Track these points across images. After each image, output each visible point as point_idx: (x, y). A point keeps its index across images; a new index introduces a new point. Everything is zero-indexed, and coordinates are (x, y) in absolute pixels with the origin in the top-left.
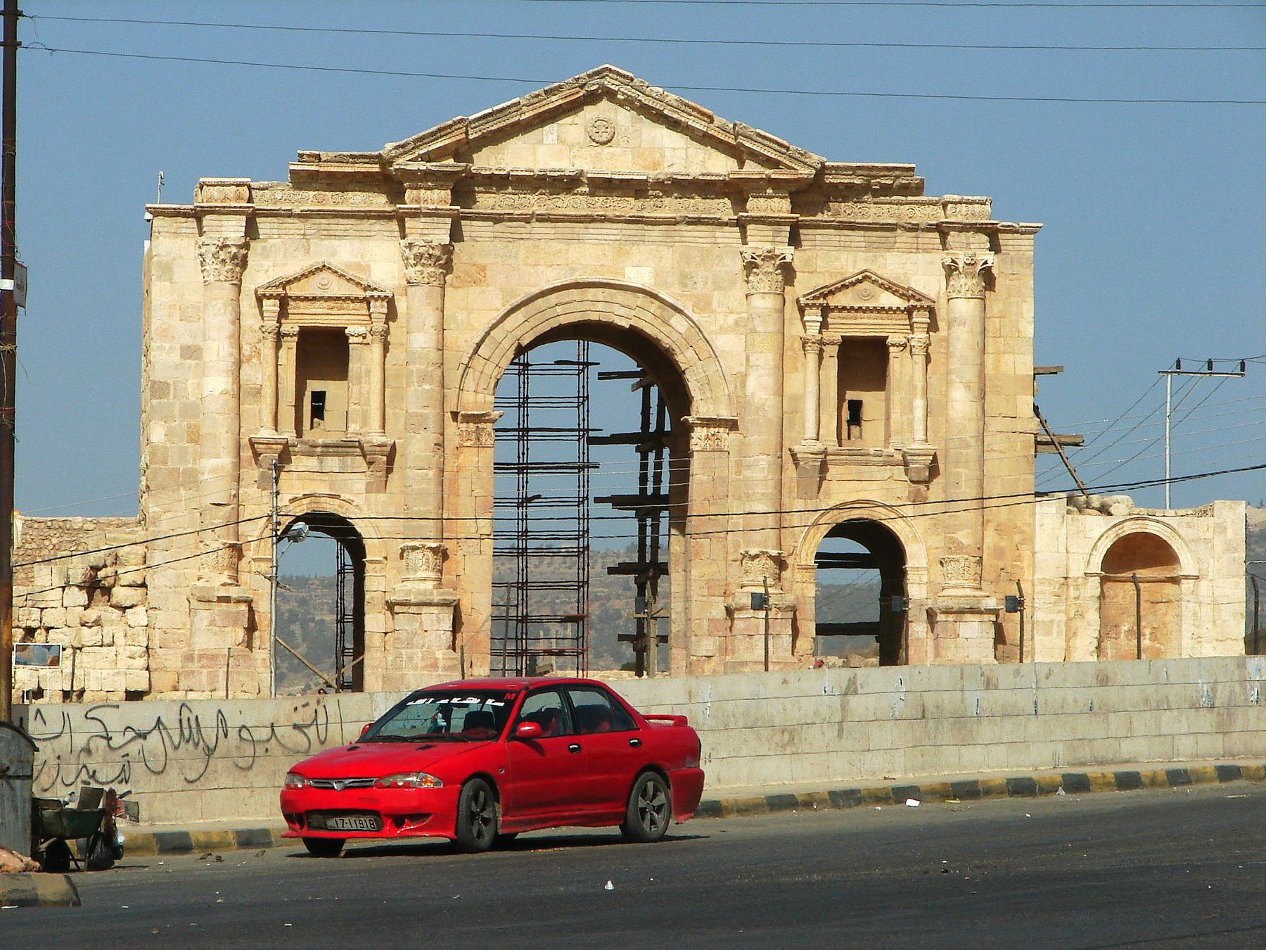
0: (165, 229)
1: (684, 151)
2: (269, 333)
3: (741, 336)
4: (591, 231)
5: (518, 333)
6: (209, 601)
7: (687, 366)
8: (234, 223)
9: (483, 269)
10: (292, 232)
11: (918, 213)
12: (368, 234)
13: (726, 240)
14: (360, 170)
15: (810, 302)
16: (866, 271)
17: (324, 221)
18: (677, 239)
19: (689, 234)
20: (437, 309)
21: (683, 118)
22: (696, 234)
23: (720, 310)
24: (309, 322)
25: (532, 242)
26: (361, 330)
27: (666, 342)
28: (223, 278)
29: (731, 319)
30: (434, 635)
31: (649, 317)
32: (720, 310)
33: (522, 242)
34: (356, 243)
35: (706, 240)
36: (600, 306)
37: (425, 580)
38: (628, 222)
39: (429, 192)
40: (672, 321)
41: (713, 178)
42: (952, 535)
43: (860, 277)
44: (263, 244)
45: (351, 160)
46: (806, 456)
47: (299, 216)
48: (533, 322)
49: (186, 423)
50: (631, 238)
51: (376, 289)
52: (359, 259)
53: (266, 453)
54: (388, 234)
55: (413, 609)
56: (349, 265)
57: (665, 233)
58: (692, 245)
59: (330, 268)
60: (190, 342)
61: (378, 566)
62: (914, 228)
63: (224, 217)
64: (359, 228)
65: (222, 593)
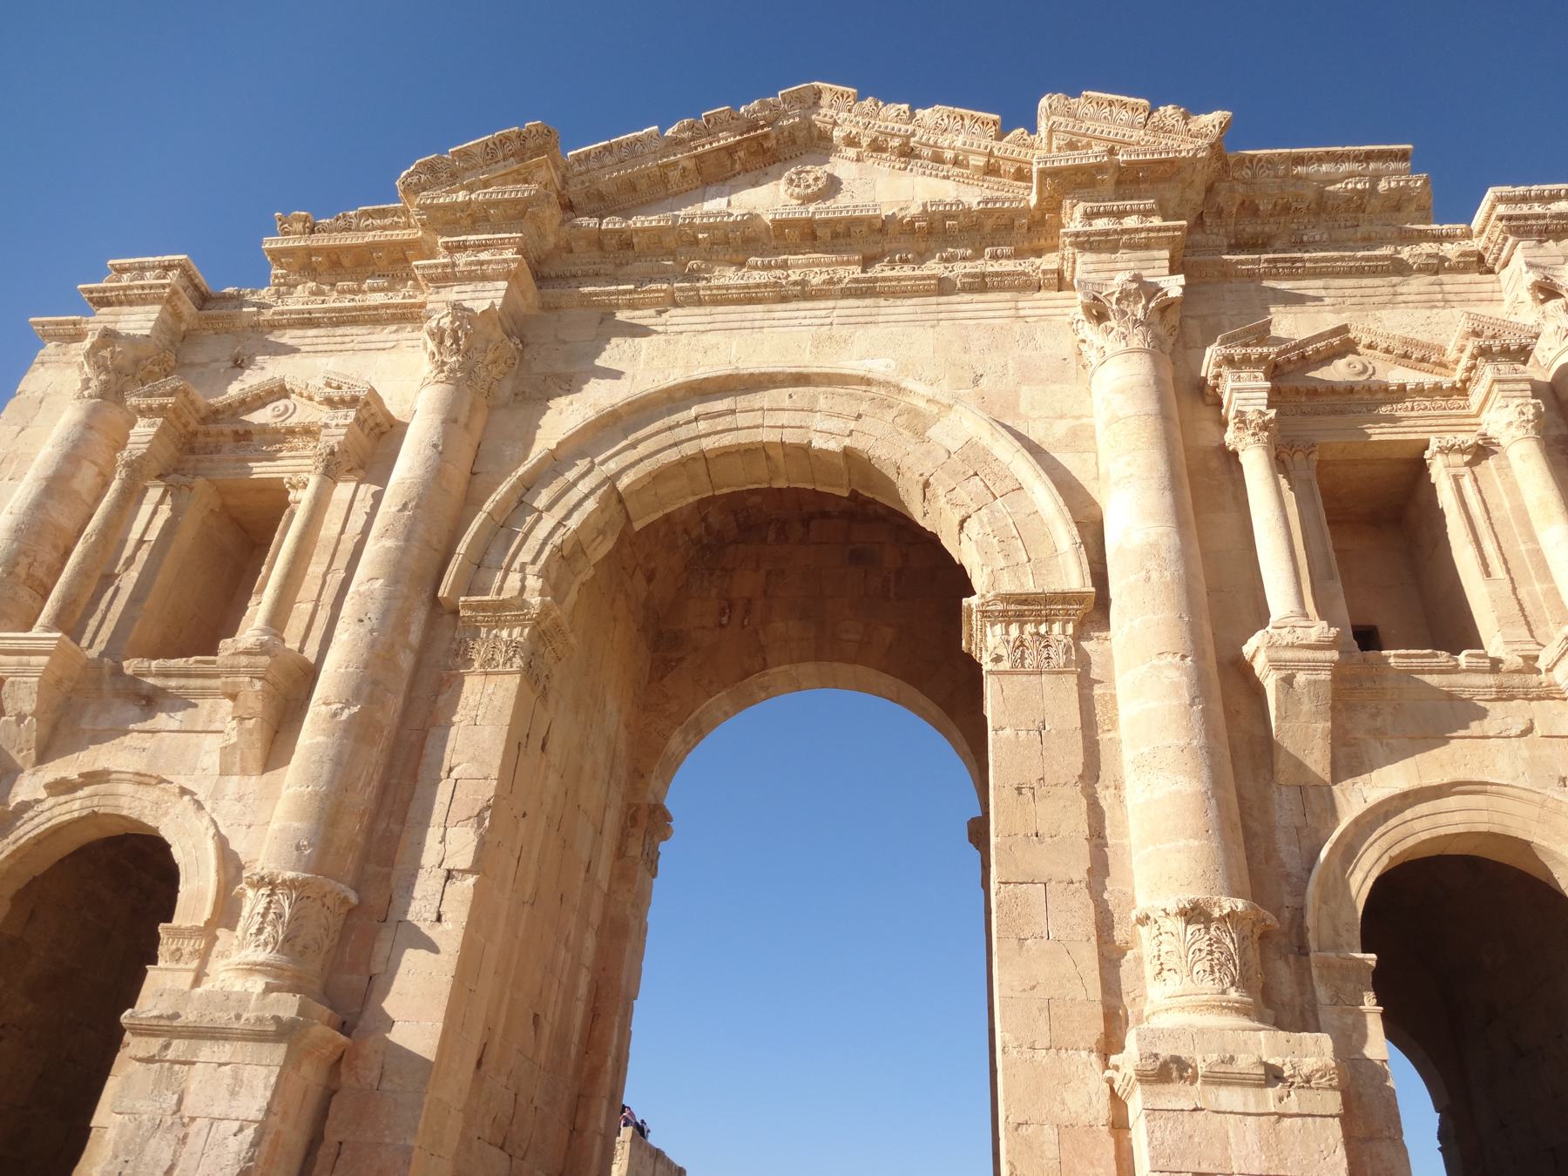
0: (53, 358)
3: (1085, 456)
4: (777, 315)
5: (612, 466)
8: (138, 317)
15: (1238, 352)
16: (1343, 329)
18: (941, 316)
21: (944, 141)
25: (662, 337)
29: (1061, 428)
36: (784, 418)
37: (252, 969)
38: (847, 294)
41: (1006, 205)
43: (1336, 341)
45: (363, 223)
46: (1288, 654)
48: (642, 449)
50: (852, 320)
51: (339, 388)
53: (14, 674)
55: (178, 1048)
57: (918, 309)
61: (188, 946)
62: (1437, 267)
63: (126, 309)
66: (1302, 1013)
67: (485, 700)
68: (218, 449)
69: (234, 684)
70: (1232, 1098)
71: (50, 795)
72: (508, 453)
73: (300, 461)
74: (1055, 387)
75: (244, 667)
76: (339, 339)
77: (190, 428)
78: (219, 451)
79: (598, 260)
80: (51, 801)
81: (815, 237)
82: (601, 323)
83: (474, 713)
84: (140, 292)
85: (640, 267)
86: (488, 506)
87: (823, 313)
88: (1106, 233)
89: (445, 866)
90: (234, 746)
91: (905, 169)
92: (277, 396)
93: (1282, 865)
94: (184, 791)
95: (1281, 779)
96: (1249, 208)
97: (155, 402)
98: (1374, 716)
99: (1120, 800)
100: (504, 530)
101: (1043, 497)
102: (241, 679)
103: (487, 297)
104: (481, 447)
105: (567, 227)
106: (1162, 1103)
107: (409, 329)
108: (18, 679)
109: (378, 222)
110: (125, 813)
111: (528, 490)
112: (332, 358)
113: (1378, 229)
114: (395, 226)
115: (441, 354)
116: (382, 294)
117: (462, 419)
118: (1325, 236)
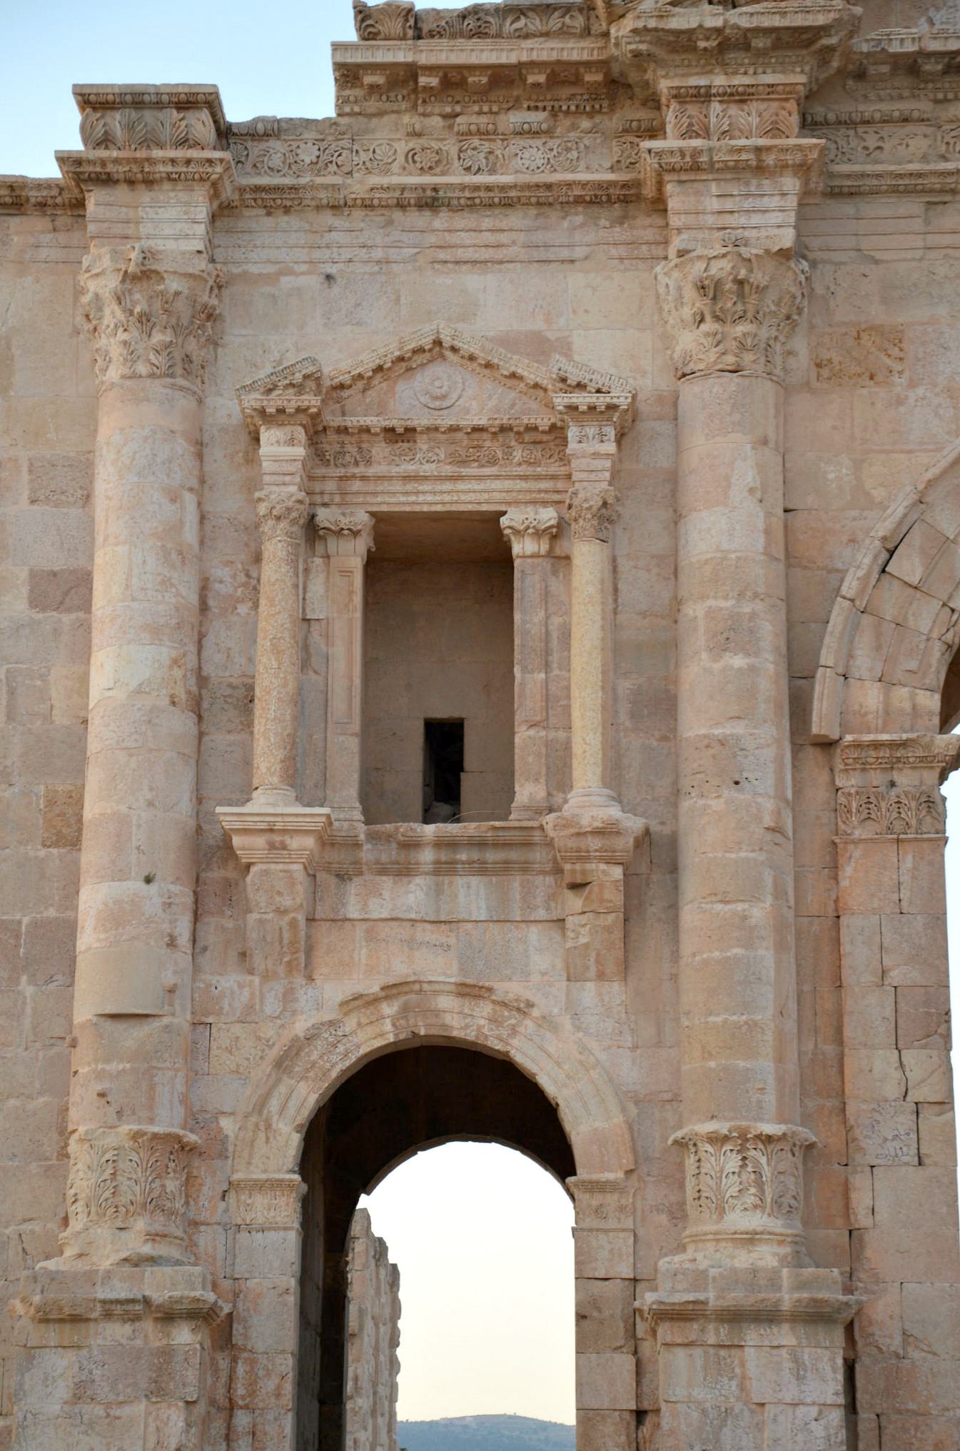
2: (278, 518)
6: (76, 1319)
8: (173, 213)
9: (893, 338)
10: (346, 254)
12: (565, 254)
14: (535, 56)
20: (765, 442)
24: (399, 499)
26: (548, 516)
28: (142, 368)
39: (733, 110)
44: (268, 289)
45: (508, 27)
47: (368, 206)
51: (580, 386)
52: (539, 325)
54: (622, 251)
56: (509, 342)
59: (454, 349)
60: (58, 562)
61: (611, 1200)
63: (145, 196)
64: (539, 237)
65: (120, 1290)
69: (584, 872)
71: (346, 1014)
72: (832, 476)
73: (507, 484)
75: (596, 851)
76: (489, 238)
78: (369, 462)
79: (906, 93)
80: (350, 1024)
83: (896, 897)
84: (169, 169)
86: (850, 586)
89: (914, 1096)
90: (586, 946)
94: (530, 1005)
97: (291, 401)
100: (866, 620)
102: (593, 866)
104: (788, 465)
107: (603, 222)
108: (273, 866)
109: (535, 24)
110: (455, 1034)
111: (891, 553)
112: (489, 276)
114: (563, 33)
116: (539, 142)
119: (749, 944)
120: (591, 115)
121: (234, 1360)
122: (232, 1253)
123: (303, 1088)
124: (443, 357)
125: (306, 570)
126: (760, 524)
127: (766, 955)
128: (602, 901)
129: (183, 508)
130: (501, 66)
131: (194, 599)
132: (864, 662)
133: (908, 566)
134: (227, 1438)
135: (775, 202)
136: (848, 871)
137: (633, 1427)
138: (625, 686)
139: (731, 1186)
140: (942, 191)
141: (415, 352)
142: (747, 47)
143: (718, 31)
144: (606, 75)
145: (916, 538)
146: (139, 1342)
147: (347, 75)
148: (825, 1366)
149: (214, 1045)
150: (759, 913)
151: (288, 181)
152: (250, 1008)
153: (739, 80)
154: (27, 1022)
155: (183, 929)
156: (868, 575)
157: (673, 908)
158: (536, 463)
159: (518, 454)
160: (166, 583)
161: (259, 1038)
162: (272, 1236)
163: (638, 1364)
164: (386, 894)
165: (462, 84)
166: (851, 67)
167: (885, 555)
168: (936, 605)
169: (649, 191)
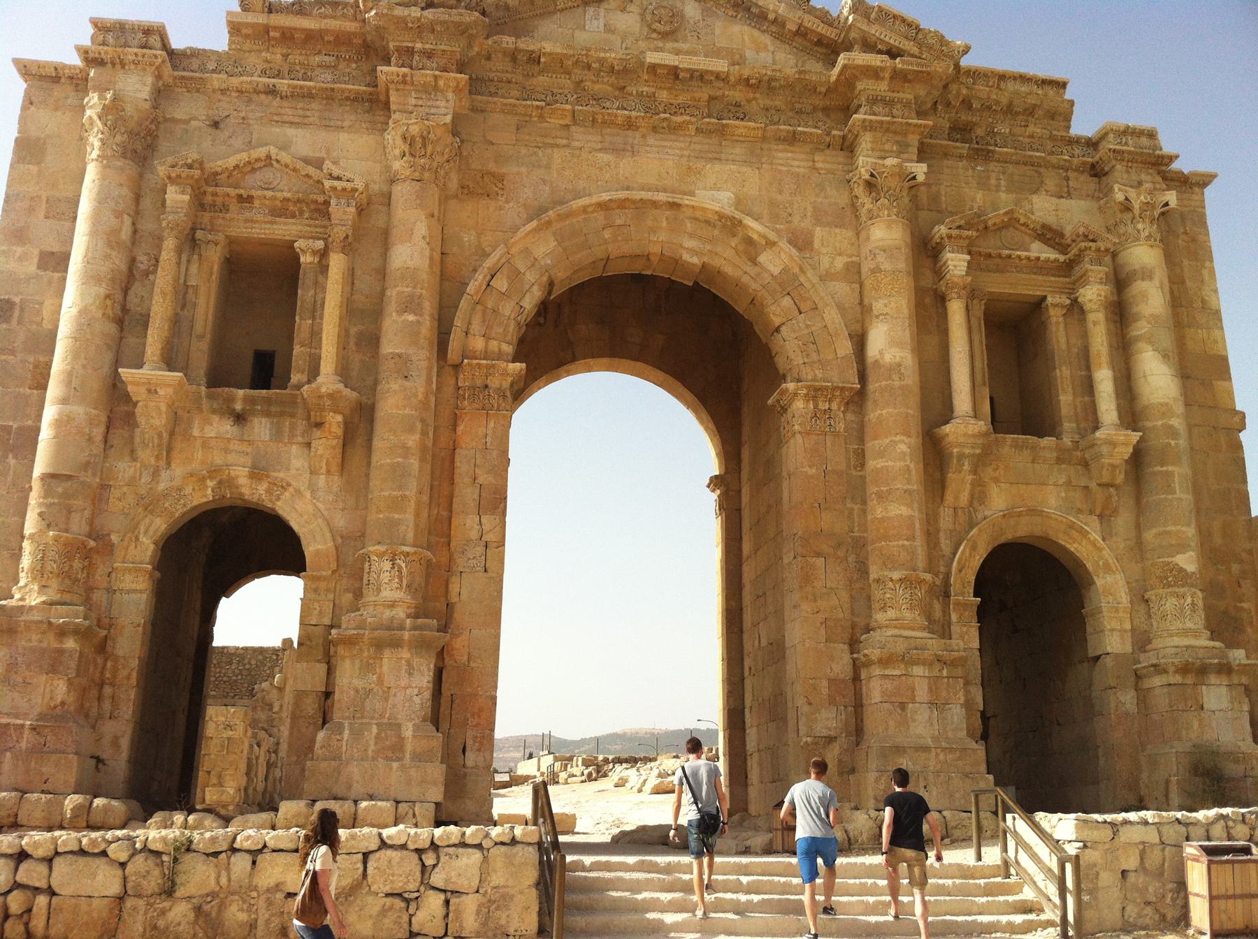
1: (770, 54)
7: (784, 320)
9: (500, 178)
11: (1065, 151)
13: (828, 166)
15: (955, 232)
16: (1011, 212)
17: (276, 102)
19: (781, 155)
20: (433, 216)
22: (790, 155)
23: (824, 250)
25: (567, 152)
26: (320, 244)
27: (754, 286)
29: (840, 263)
30: (400, 696)
31: (729, 253)
32: (824, 250)
33: (556, 150)
34: (323, 136)
35: (802, 164)
40: (762, 258)
42: (1170, 559)
44: (185, 126)
46: (962, 440)
49: (32, 360)
51: (339, 178)
58: (784, 169)
59: (278, 161)
60: (56, 248)
61: (323, 585)
66: (943, 626)
67: (489, 432)
68: (225, 208)
70: (918, 670)
74: (837, 230)
76: (301, 112)
77: (202, 190)
81: (677, 77)
82: (518, 129)
85: (543, 81)
86: (471, 288)
87: (682, 145)
88: (882, 122)
90: (321, 456)
91: (736, 16)
92: (263, 163)
93: (941, 551)
95: (946, 504)
96: (967, 104)
98: (995, 470)
99: (864, 512)
100: (479, 307)
101: (832, 316)
103: (444, 110)
105: (490, 41)
106: (887, 672)
111: (493, 277)
113: (1039, 131)
115: (412, 155)
117: (436, 214)
118: (1008, 130)
119: (405, 457)
120: (356, 62)
121: (106, 660)
122: (110, 604)
123: (158, 521)
124: (272, 165)
125: (189, 261)
126: (427, 252)
127: (414, 463)
128: (330, 432)
129: (122, 222)
130: (311, 30)
131: (124, 267)
132: (476, 326)
133: (501, 283)
134: (99, 699)
135: (443, 104)
136: (460, 428)
137: (323, 699)
138: (353, 330)
139: (385, 577)
140: (526, 115)
141: (256, 160)
142: (433, 31)
143: (419, 19)
144: (364, 41)
145: (505, 270)
146: (44, 645)
147: (235, 29)
148: (424, 668)
149: (111, 496)
150: (413, 440)
151: (197, 75)
152: (133, 479)
153: (427, 46)
154: (10, 478)
155: (98, 432)
156: (480, 285)
157: (369, 441)
158: (316, 219)
159: (306, 215)
160: (107, 257)
161: (137, 494)
162: (134, 596)
163: (329, 669)
164: (215, 425)
165: (292, 38)
166: (483, 52)
167: (489, 277)
168: (513, 303)
169: (382, 97)
